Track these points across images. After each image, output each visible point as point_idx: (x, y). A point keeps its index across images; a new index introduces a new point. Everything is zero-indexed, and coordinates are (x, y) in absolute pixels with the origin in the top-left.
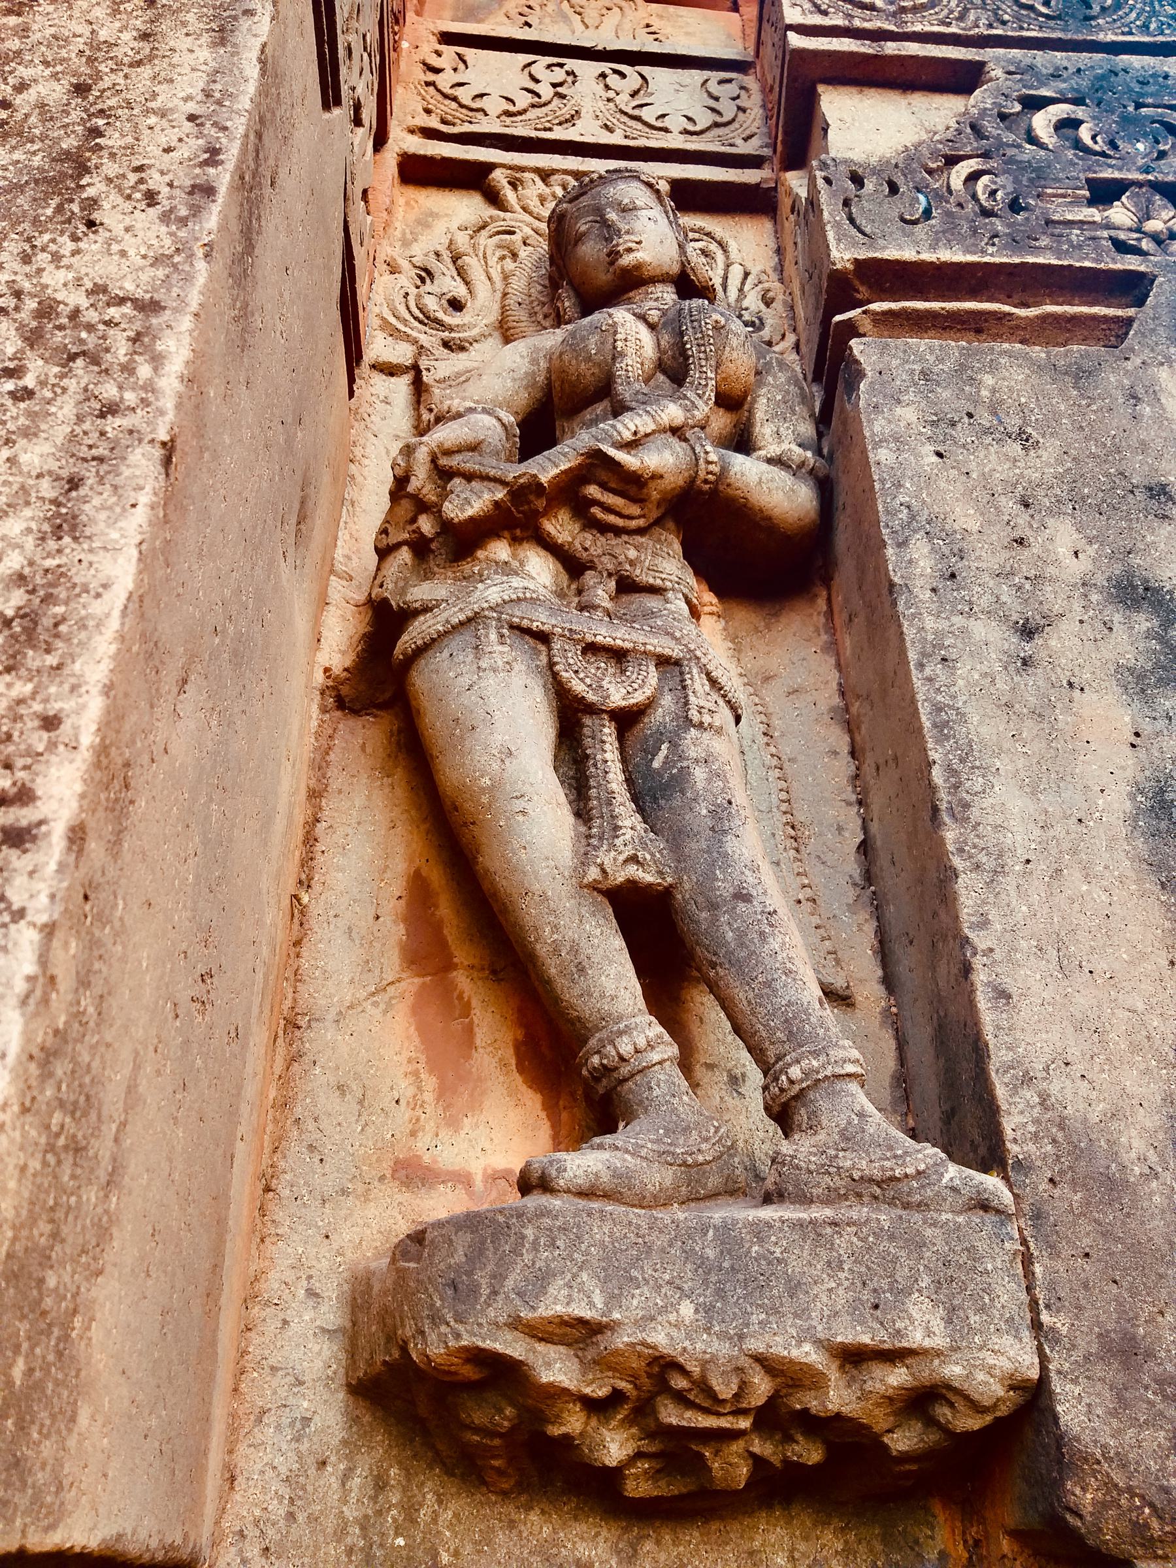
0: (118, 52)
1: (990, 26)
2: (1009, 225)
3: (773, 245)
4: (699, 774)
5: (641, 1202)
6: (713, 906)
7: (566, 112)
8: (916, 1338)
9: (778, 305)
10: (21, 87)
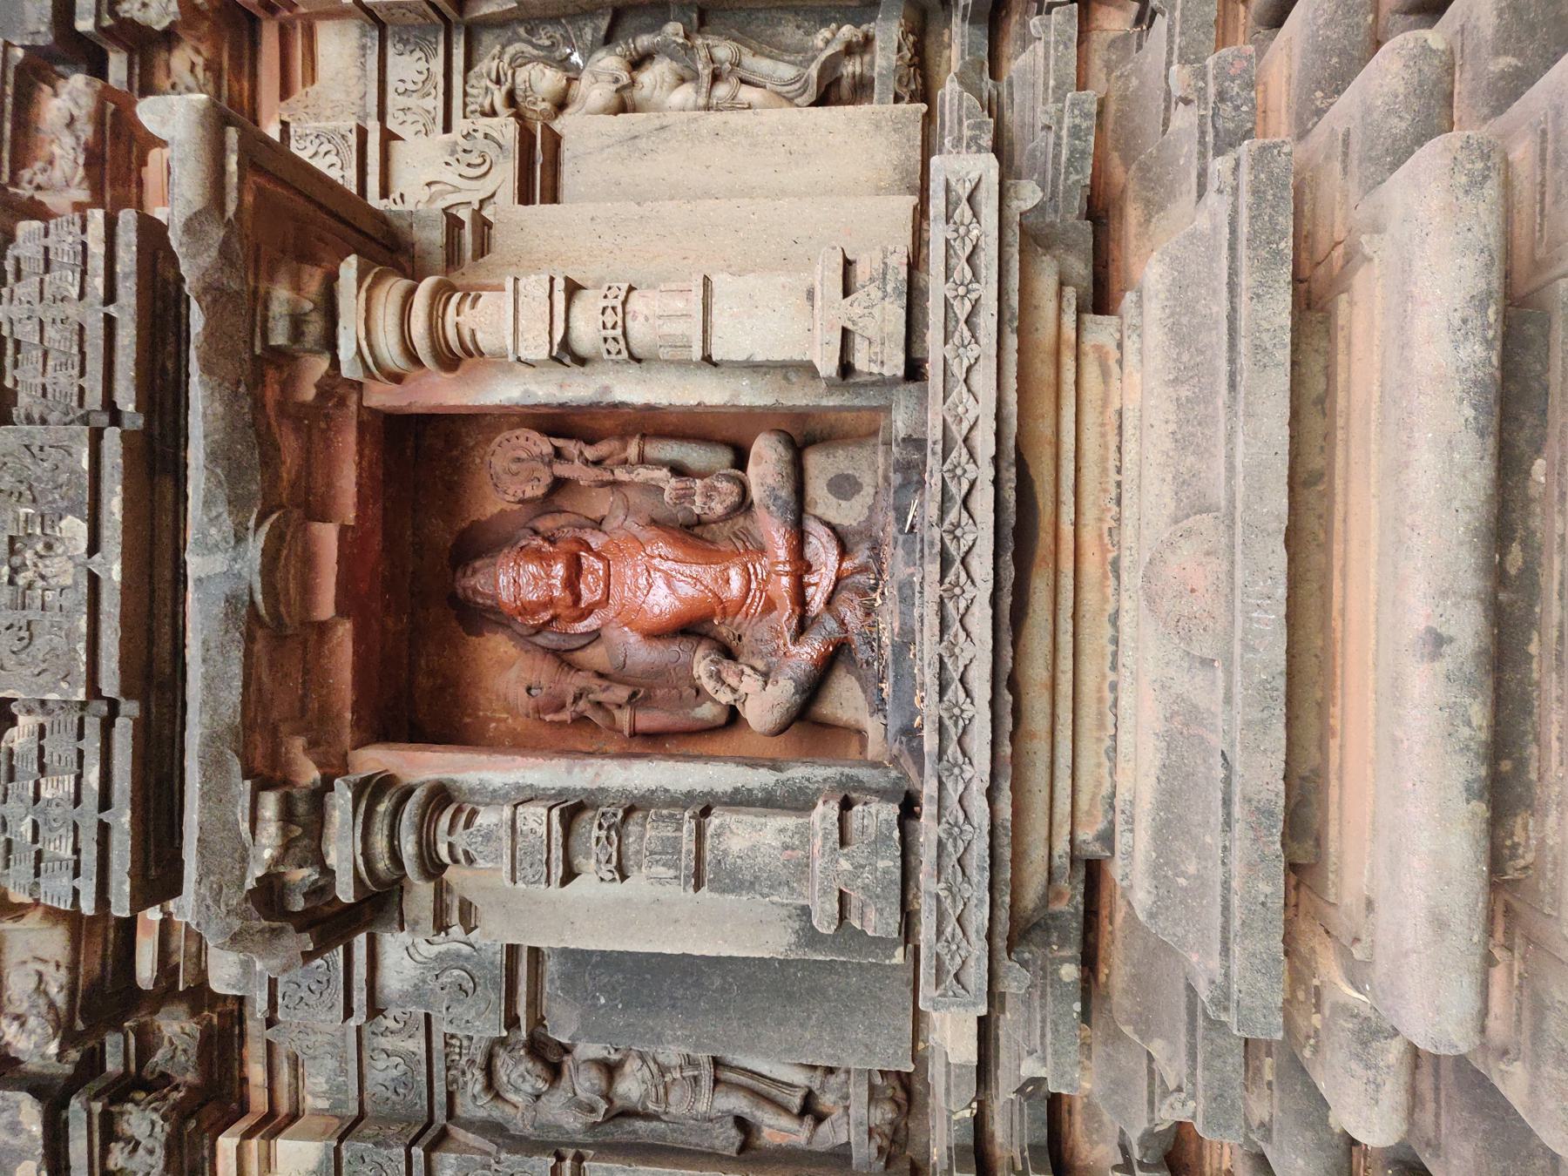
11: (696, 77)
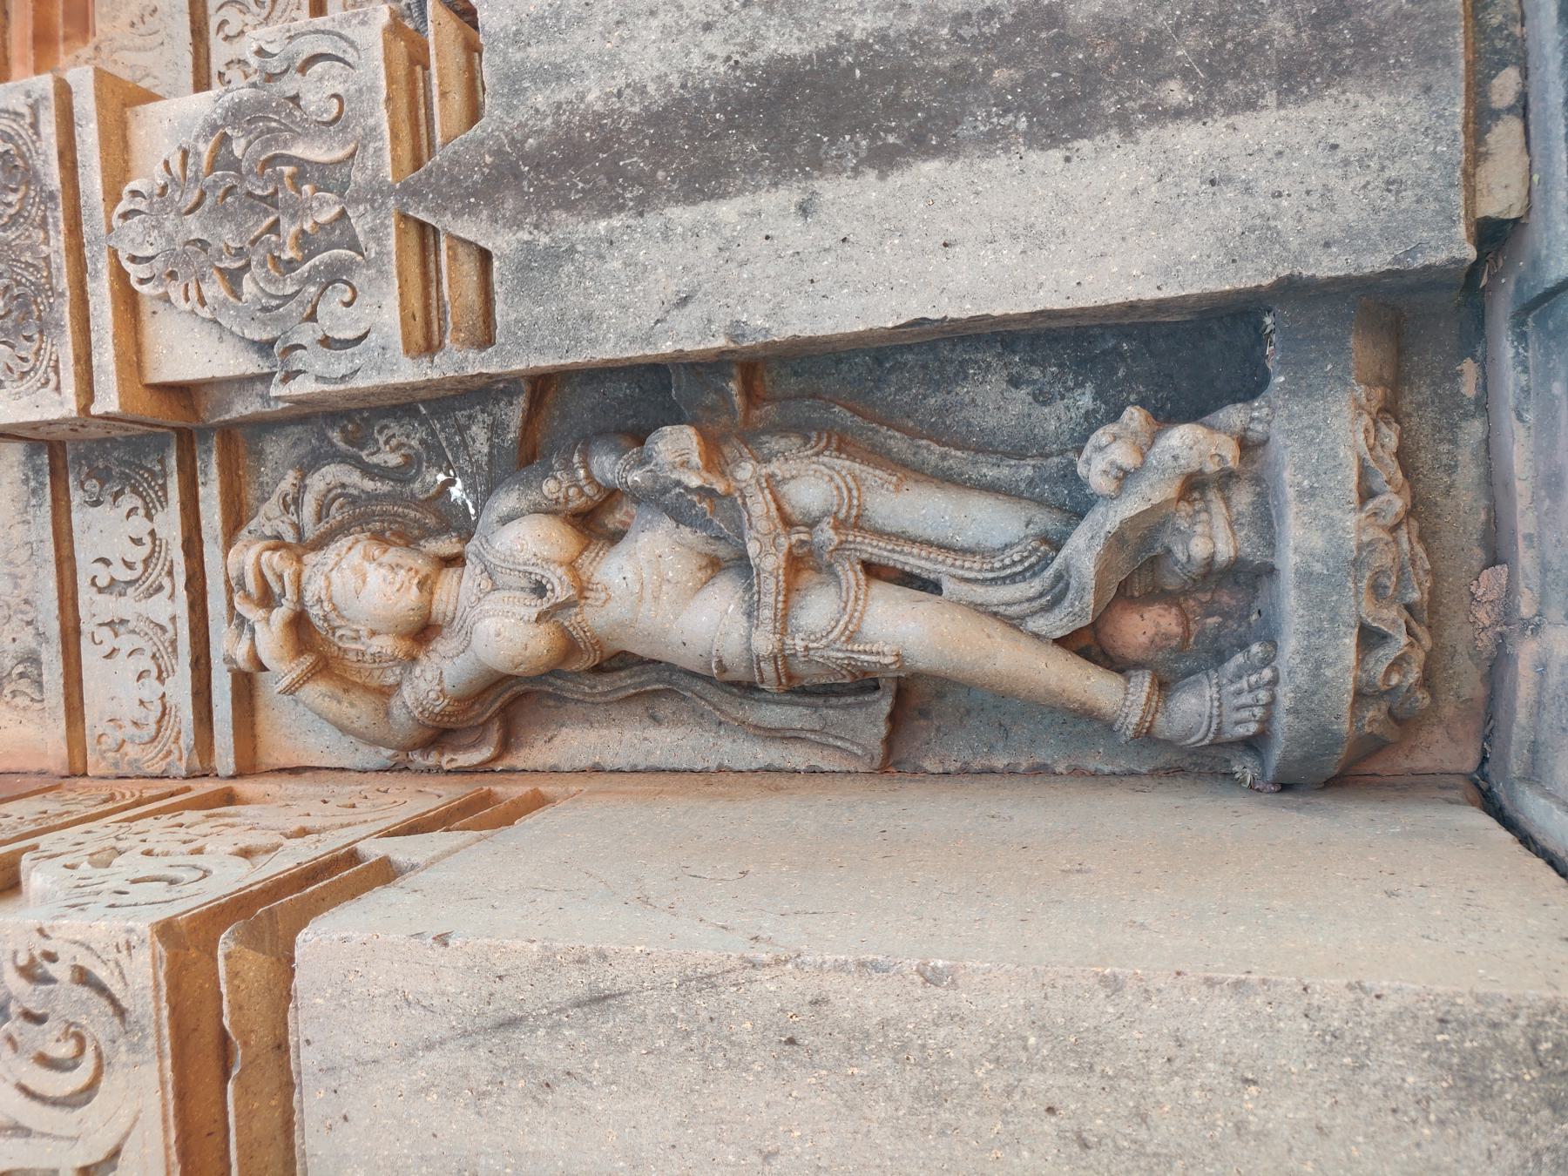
0: (669, 20)
10: (712, 57)
11: (742, 565)
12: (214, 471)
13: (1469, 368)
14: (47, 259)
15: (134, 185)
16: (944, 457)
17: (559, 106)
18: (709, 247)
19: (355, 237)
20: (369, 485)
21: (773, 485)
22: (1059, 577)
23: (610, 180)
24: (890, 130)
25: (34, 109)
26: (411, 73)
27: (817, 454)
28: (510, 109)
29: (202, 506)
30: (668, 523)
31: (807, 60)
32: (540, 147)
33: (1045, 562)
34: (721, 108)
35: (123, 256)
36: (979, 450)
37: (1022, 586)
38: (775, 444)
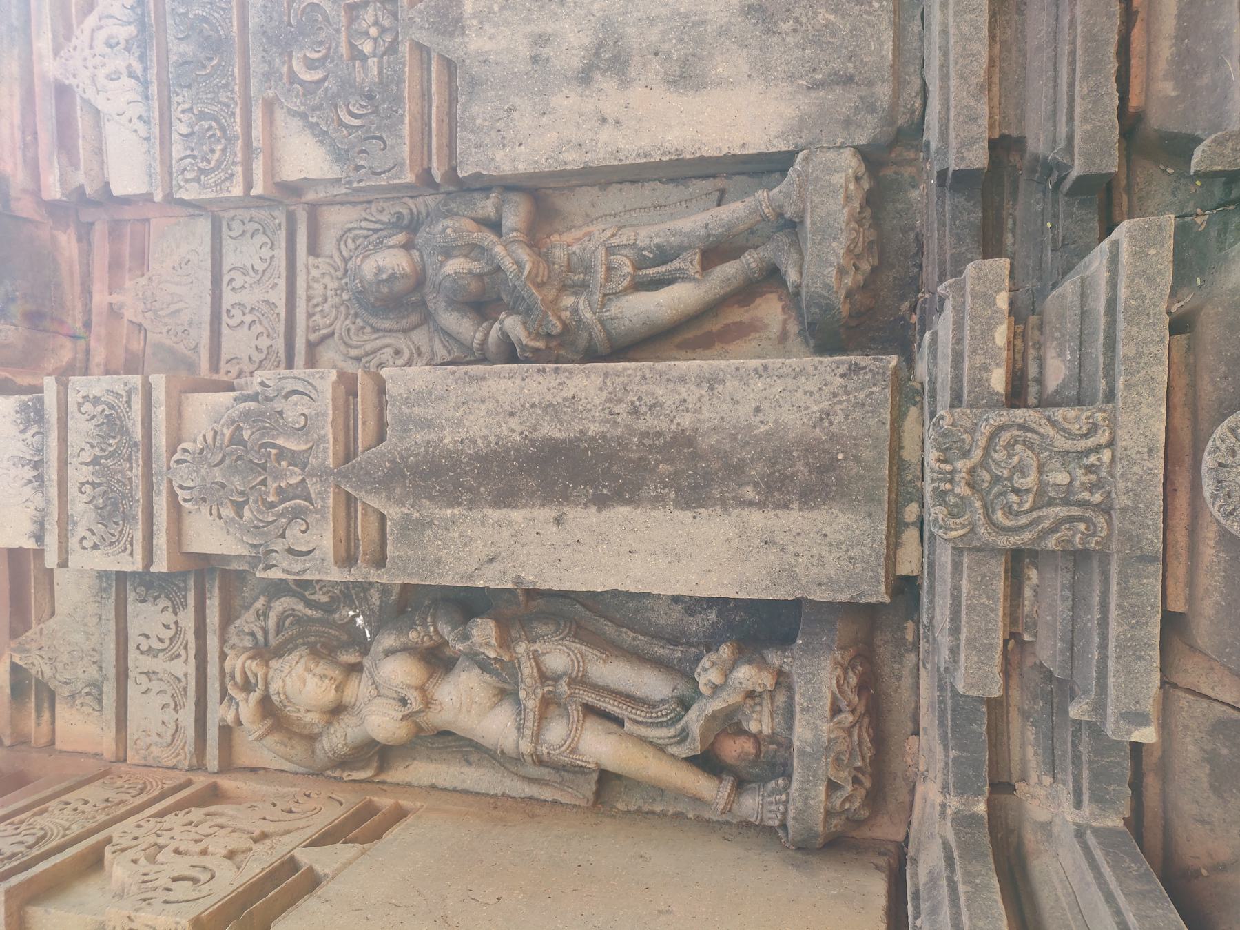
0: (491, 407)
1: (232, 91)
2: (384, 102)
3: (339, 206)
4: (657, 240)
5: (802, 259)
6: (709, 236)
7: (264, 308)
8: (842, 181)
9: (385, 205)
10: (513, 431)
12: (216, 591)
13: (910, 625)
14: (130, 479)
15: (184, 445)
16: (634, 639)
17: (428, 442)
18: (506, 533)
19: (309, 493)
20: (309, 612)
21: (536, 657)
22: (683, 730)
23: (455, 488)
24: (605, 487)
25: (129, 393)
26: (347, 401)
27: (562, 639)
28: (401, 439)
29: (208, 611)
30: (477, 671)
31: (563, 441)
32: (417, 463)
33: (679, 718)
34: (516, 459)
35: (175, 485)
36: (653, 637)
37: (665, 730)
38: (541, 629)
